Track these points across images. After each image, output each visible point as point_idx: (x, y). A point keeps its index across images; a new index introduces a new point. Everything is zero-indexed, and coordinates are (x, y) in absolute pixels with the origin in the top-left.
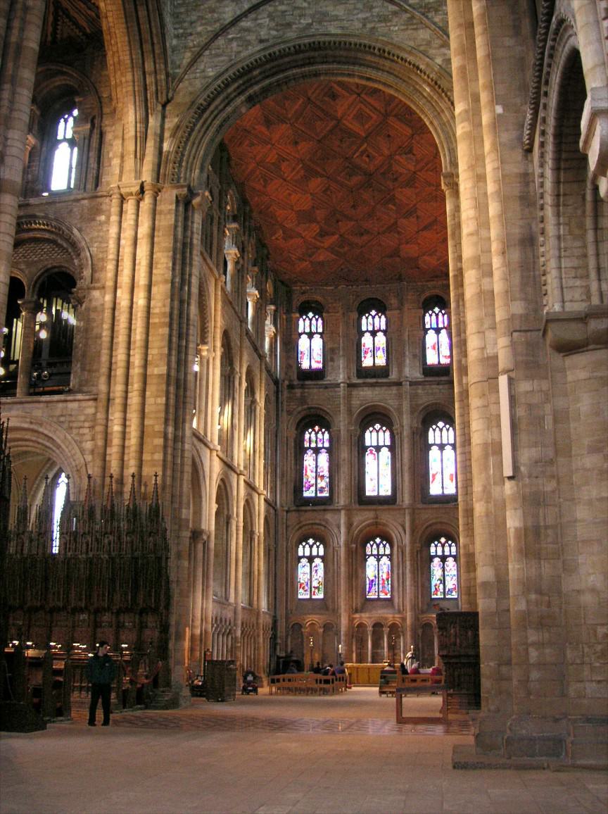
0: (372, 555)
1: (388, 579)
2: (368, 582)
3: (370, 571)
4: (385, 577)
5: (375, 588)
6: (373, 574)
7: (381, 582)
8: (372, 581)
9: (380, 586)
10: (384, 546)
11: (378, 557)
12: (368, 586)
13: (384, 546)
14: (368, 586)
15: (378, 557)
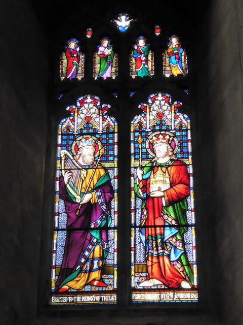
0: (91, 85)
1: (177, 201)
2: (61, 220)
3: (81, 165)
4: (160, 185)
5: (103, 248)
6: (94, 177)
7: (137, 218)
8: (90, 208)
9: (138, 238)
10: (158, 48)
11: (124, 98)
12: (59, 239)
13: (158, 48)
14: (59, 239)
15: (124, 98)
